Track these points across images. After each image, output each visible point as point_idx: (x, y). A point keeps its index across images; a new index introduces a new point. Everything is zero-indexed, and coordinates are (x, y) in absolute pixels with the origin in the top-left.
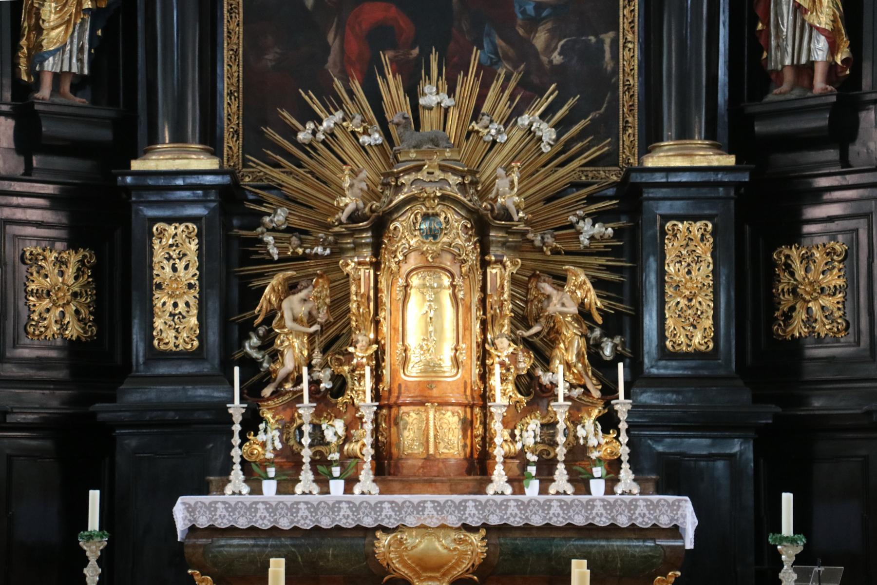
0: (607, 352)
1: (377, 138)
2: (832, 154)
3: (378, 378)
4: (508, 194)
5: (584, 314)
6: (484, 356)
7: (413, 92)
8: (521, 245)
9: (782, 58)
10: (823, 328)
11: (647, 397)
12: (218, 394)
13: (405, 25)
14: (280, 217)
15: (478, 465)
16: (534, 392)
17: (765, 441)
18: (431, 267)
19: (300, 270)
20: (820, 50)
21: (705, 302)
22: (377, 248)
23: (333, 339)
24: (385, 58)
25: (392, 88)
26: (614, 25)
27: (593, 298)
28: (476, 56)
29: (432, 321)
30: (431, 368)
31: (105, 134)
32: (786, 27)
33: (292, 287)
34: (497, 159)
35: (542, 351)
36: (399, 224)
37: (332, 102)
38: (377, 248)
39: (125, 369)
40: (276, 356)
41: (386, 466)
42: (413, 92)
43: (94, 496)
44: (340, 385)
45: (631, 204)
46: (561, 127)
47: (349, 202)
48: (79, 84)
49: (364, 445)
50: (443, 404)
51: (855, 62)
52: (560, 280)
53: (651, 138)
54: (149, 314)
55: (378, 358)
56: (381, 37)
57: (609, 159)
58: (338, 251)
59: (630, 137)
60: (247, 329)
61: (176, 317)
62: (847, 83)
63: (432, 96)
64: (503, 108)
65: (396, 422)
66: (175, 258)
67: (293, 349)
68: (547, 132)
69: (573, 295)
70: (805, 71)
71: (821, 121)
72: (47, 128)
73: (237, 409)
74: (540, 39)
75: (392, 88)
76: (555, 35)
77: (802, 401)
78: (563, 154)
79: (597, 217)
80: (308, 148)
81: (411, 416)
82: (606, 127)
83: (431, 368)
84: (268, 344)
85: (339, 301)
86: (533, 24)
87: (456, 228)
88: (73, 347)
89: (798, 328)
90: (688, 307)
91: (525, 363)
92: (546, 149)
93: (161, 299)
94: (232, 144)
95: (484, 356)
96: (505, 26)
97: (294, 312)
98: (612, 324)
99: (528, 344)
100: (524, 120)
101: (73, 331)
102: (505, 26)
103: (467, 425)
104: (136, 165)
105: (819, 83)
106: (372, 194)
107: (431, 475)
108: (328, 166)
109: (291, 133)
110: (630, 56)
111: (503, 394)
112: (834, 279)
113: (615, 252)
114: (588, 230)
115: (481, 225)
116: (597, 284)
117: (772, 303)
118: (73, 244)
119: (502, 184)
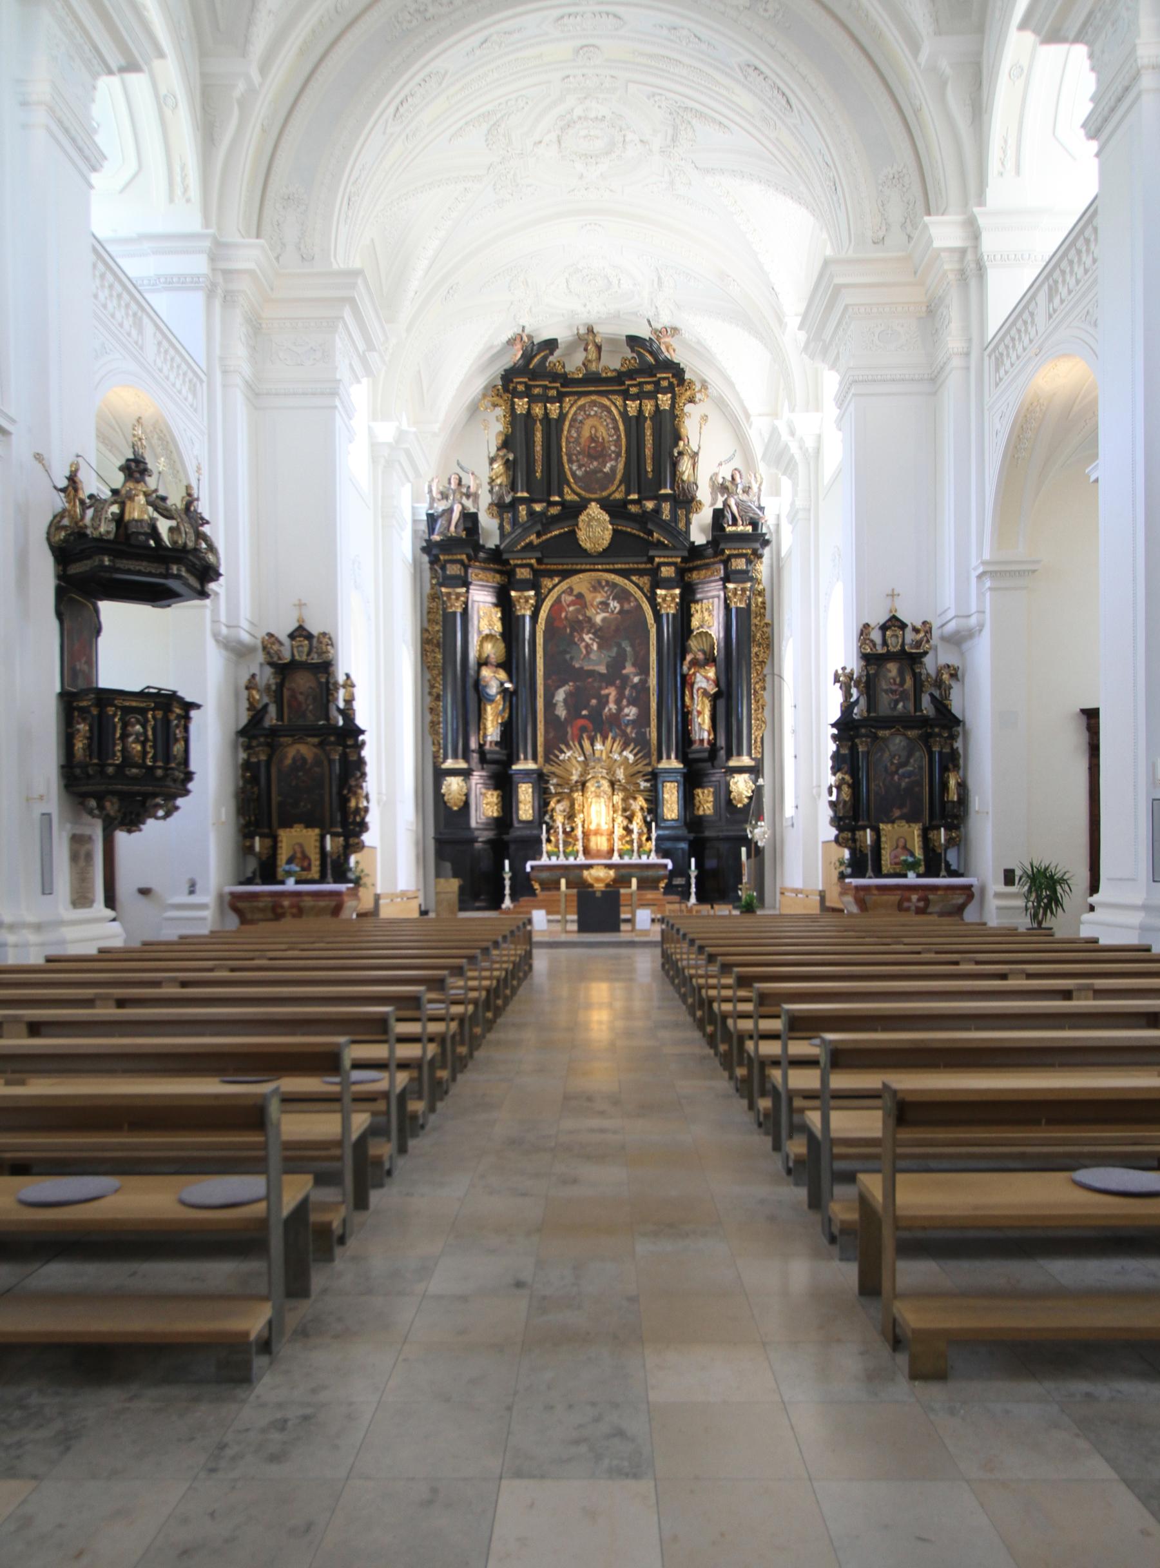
0: (649, 819)
1: (581, 759)
2: (709, 764)
3: (583, 826)
4: (620, 774)
5: (642, 809)
6: (613, 821)
7: (592, 745)
8: (624, 789)
9: (696, 736)
10: (708, 812)
11: (660, 832)
12: (535, 832)
13: (590, 726)
14: (555, 781)
15: (611, 852)
16: (629, 831)
17: (692, 844)
18: (598, 796)
19: (561, 798)
20: (705, 735)
21: (675, 806)
22: (583, 791)
23: (571, 816)
24: (585, 736)
25: (586, 744)
26: (649, 726)
27: (645, 806)
28: (610, 735)
29: (599, 812)
30: (598, 825)
31: (505, 758)
32: (697, 728)
33: (559, 802)
34: (617, 764)
35: (630, 819)
36: (588, 784)
37: (569, 747)
38: (583, 791)
39: (511, 825)
40: (554, 821)
41: (586, 852)
42: (592, 745)
43: (507, 862)
44: (573, 829)
45: (654, 777)
46: (635, 755)
47: (575, 778)
48: (497, 743)
49: (579, 846)
50: (602, 835)
51: (715, 739)
52: (635, 799)
53: (660, 758)
54: (518, 809)
55: (584, 821)
56: (583, 729)
57: (649, 764)
58: (572, 791)
59: (654, 758)
60: (546, 813)
61: (525, 810)
62: (713, 745)
63: (598, 746)
64: (619, 750)
65: (588, 840)
66: (525, 792)
67: (559, 820)
68: (631, 757)
69: (640, 803)
70: (702, 741)
71: (706, 755)
72: (488, 756)
73: (544, 836)
74: (629, 730)
75: (586, 744)
76: (633, 728)
77: (703, 832)
78: (636, 763)
79: (646, 781)
80: (563, 761)
81: (593, 839)
82: (648, 755)
83: (598, 825)
84: (552, 817)
85: (572, 805)
86: (627, 725)
87: (605, 785)
88: (496, 819)
89: (701, 812)
90: (671, 808)
91: (625, 823)
92: (631, 761)
93: (521, 806)
94: (540, 759)
95: (613, 821)
96: (619, 727)
97: (559, 809)
98: (650, 811)
99: (627, 817)
100: (625, 753)
101: (495, 814)
102: (619, 727)
103: (609, 840)
104: (514, 767)
105: (706, 745)
106: (581, 775)
107: (599, 854)
108: (568, 766)
109: (557, 757)
110: (654, 735)
111: (619, 831)
112: (711, 799)
113: (650, 791)
114: (644, 785)
115: (612, 784)
116: (646, 800)
117: (694, 805)
118: (496, 789)
119: (618, 772)
